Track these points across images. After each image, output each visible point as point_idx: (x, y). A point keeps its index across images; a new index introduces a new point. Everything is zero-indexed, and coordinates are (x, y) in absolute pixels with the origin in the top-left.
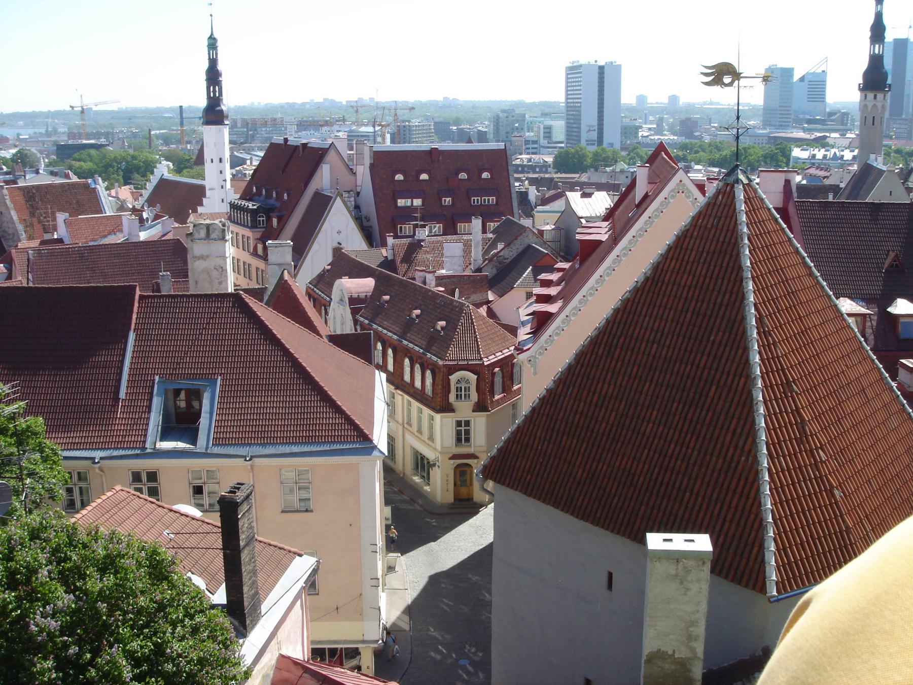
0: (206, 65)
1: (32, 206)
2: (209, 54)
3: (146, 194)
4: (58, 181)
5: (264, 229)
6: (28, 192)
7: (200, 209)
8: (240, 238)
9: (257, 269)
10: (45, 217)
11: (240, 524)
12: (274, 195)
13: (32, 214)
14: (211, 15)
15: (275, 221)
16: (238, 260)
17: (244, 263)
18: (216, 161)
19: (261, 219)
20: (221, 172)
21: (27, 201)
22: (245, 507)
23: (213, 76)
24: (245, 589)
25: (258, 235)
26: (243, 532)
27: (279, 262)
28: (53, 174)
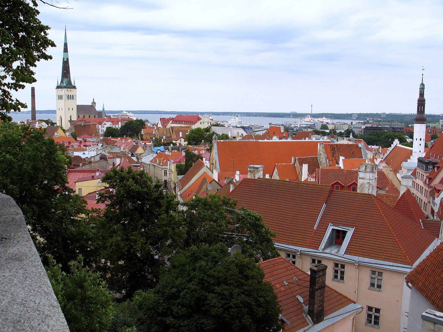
0: (418, 96)
1: (333, 152)
2: (420, 92)
3: (388, 152)
4: (350, 143)
5: (431, 172)
6: (332, 147)
7: (408, 161)
8: (421, 174)
9: (425, 190)
10: (338, 158)
11: (317, 280)
12: (438, 157)
13: (333, 156)
14: (423, 75)
15: (436, 168)
16: (419, 185)
17: (421, 186)
18: (419, 139)
19: (430, 167)
20: (420, 145)
21: (331, 150)
22: (321, 274)
23: (421, 103)
24: (316, 306)
25: (428, 175)
26: (318, 283)
27: (406, 185)
28: (350, 140)
